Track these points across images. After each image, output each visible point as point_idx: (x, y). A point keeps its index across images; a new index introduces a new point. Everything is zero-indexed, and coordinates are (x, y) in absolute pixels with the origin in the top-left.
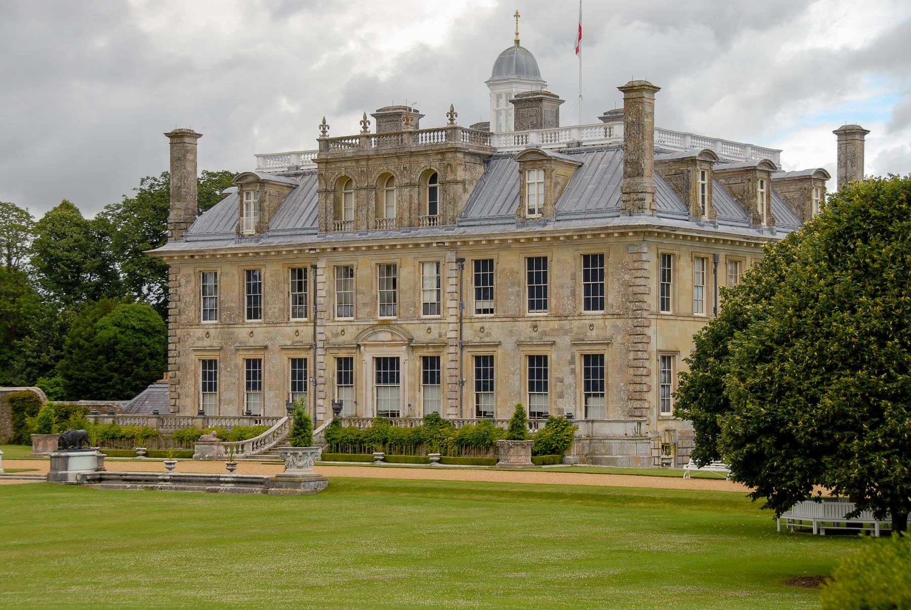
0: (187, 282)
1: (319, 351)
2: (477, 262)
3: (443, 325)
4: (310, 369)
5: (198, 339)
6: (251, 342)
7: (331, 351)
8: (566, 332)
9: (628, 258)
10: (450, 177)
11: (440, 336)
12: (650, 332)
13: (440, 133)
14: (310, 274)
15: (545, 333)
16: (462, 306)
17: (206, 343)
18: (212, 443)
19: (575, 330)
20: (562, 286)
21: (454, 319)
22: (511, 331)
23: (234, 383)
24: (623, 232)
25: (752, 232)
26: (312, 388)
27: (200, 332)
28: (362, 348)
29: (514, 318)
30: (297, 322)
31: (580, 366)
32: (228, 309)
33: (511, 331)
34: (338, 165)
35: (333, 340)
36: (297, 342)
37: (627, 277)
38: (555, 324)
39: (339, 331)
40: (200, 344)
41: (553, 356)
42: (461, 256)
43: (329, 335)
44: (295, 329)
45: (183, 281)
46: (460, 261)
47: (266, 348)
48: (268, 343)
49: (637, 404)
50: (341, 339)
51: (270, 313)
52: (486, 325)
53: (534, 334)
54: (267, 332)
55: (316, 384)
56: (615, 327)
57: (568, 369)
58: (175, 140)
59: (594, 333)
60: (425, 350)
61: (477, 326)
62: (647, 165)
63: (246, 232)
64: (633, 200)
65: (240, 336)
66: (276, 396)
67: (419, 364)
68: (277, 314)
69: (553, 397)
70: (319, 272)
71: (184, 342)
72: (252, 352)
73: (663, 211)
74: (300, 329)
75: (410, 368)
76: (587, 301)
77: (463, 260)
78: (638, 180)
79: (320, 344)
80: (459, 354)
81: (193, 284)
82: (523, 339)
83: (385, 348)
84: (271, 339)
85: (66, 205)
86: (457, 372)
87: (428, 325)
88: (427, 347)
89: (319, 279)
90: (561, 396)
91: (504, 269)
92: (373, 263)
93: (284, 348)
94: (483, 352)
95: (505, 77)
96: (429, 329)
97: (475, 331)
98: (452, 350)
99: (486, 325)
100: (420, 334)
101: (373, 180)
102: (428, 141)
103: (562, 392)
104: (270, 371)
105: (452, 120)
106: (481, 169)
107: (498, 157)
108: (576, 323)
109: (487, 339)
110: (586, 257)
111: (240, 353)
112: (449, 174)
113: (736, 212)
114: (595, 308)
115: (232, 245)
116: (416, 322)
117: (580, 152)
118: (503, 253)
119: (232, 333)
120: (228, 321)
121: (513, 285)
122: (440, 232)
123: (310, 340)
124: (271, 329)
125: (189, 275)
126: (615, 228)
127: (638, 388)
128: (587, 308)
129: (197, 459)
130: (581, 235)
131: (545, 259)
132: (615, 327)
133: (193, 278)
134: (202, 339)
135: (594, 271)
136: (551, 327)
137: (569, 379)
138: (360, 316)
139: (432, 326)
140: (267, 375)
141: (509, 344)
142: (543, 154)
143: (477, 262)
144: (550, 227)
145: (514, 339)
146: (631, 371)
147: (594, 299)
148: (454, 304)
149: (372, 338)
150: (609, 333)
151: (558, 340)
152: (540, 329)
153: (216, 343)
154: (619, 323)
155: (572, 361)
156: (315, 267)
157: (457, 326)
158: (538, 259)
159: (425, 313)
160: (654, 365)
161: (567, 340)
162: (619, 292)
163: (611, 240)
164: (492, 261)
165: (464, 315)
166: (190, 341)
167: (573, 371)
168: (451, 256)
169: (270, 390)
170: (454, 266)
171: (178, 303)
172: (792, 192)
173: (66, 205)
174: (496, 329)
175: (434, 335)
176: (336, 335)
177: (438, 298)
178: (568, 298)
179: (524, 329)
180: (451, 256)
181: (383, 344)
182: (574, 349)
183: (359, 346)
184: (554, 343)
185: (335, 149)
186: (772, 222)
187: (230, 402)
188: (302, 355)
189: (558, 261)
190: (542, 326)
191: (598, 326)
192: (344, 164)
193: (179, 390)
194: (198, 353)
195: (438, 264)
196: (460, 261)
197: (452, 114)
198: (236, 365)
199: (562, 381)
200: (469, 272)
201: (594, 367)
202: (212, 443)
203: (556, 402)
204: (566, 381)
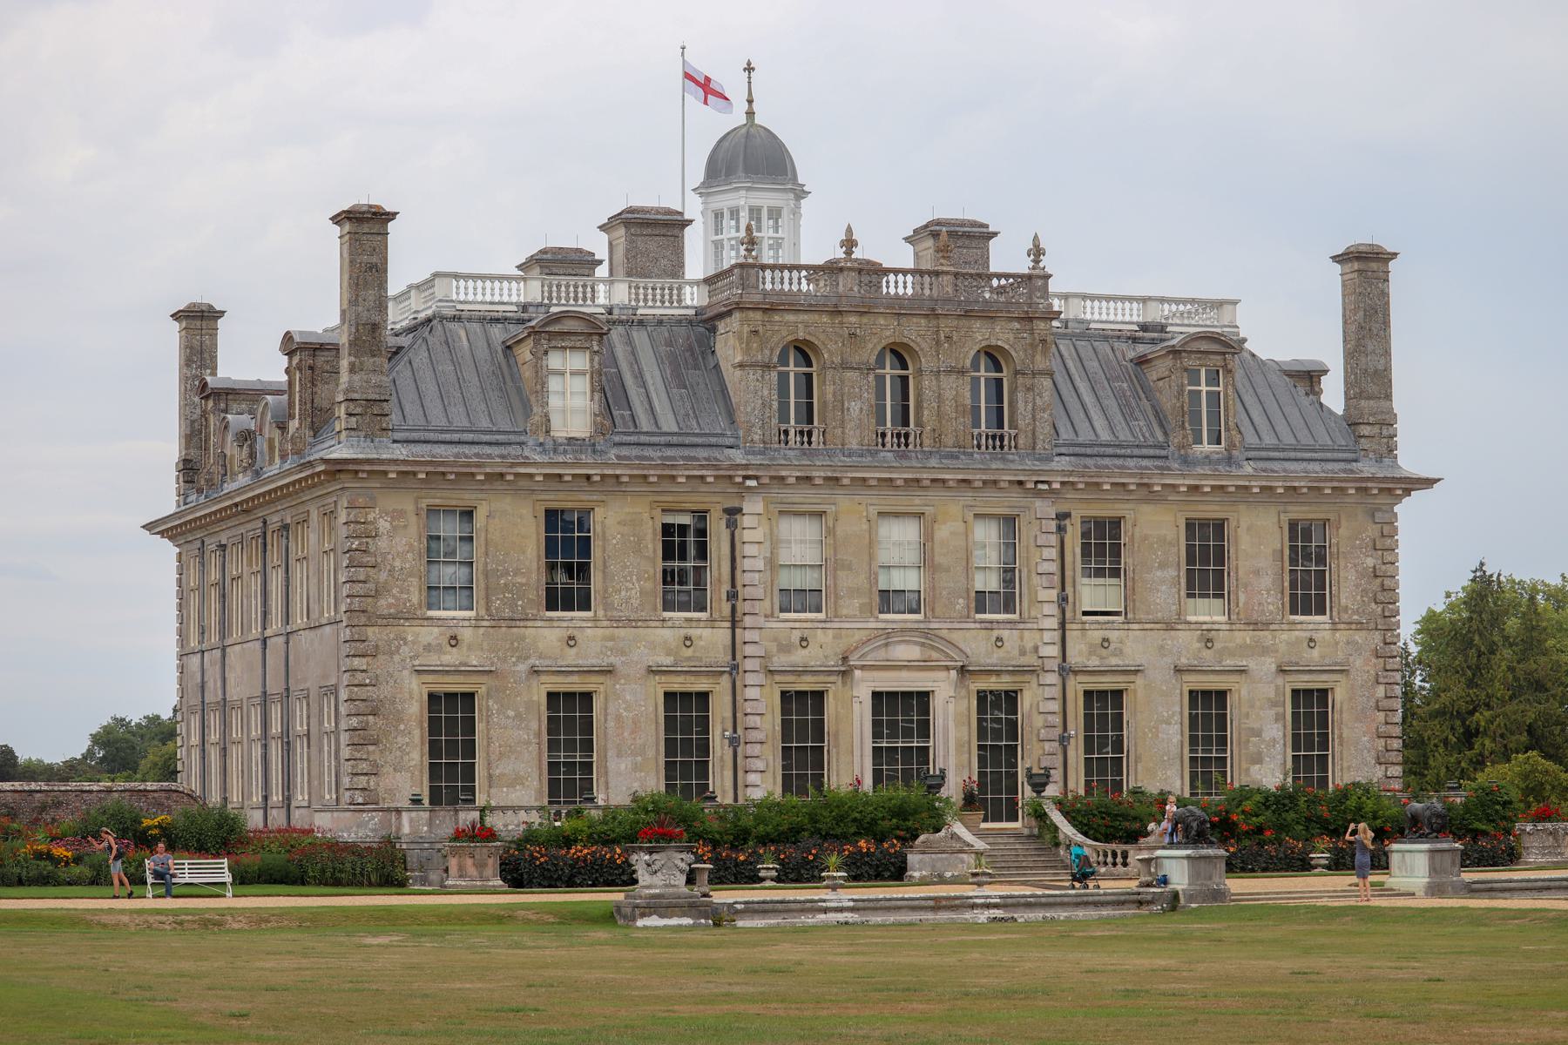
0: (394, 528)
3: (1026, 633)
5: (428, 648)
6: (571, 657)
7: (778, 678)
8: (1265, 651)
9: (1372, 531)
11: (1023, 653)
13: (795, 274)
16: (1063, 599)
17: (451, 658)
19: (1283, 648)
20: (1257, 573)
21: (1053, 623)
22: (1162, 647)
23: (528, 743)
26: (729, 752)
27: (429, 634)
28: (857, 673)
29: (1169, 627)
30: (687, 620)
33: (1162, 647)
34: (790, 317)
35: (779, 661)
36: (689, 659)
37: (1370, 562)
38: (1246, 637)
39: (796, 636)
40: (433, 660)
42: (1064, 508)
43: (773, 647)
44: (683, 632)
45: (384, 525)
46: (1063, 516)
47: (608, 672)
48: (612, 659)
50: (799, 657)
51: (616, 599)
52: (1113, 635)
53: (1207, 654)
54: (612, 638)
55: (734, 742)
58: (366, 228)
59: (1316, 653)
60: (993, 679)
61: (1096, 636)
65: (540, 645)
66: (636, 768)
68: (635, 602)
69: (1244, 766)
70: (747, 521)
71: (392, 654)
72: (575, 678)
74: (693, 632)
77: (1067, 515)
78: (1383, 403)
79: (749, 665)
80: (1059, 688)
81: (413, 530)
82: (1184, 661)
83: (904, 674)
86: (1057, 720)
87: (995, 633)
88: (998, 673)
89: (748, 535)
91: (1145, 538)
93: (652, 671)
94: (1106, 683)
96: (999, 639)
97: (1091, 645)
101: (869, 353)
102: (927, 292)
103: (1260, 753)
104: (619, 718)
105: (1037, 261)
108: (1285, 636)
109: (1114, 661)
110: (1293, 525)
111: (544, 678)
112: (1038, 358)
116: (972, 626)
118: (1146, 508)
119: (523, 638)
120: (507, 613)
121: (1162, 566)
123: (724, 658)
124: (622, 632)
125: (401, 514)
133: (413, 519)
134: (439, 649)
136: (1238, 641)
138: (938, 611)
139: (1005, 634)
140: (611, 724)
145: (1169, 661)
146: (1381, 716)
148: (1053, 594)
149: (882, 654)
150: (1340, 656)
151: (1251, 664)
152: (1218, 645)
154: (1359, 637)
156: (733, 513)
157: (1056, 636)
161: (1269, 664)
162: (1357, 586)
165: (1068, 615)
166: (405, 650)
168: (1046, 509)
169: (619, 755)
170: (1053, 526)
171: (371, 571)
174: (1134, 646)
176: (785, 648)
178: (1268, 591)
179: (1185, 644)
180: (1046, 509)
182: (1280, 681)
183: (846, 674)
184: (1242, 672)
187: (516, 781)
188: (700, 685)
189: (1249, 529)
192: (805, 317)
193: (377, 757)
194: (430, 678)
197: (849, 244)
203: (1248, 770)
204: (1267, 736)
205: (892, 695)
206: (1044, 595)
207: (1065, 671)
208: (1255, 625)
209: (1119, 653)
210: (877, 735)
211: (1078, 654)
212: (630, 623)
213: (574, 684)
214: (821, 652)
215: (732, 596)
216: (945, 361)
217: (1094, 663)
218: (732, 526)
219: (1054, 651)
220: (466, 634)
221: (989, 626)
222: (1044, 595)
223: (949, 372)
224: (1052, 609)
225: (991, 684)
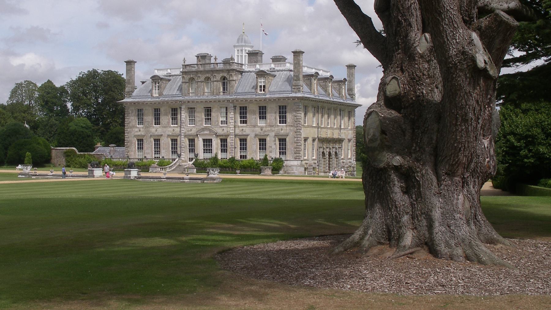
1: (182, 137)
2: (241, 107)
4: (178, 142)
6: (156, 133)
8: (273, 131)
10: (231, 79)
12: (301, 131)
14: (179, 110)
15: (265, 131)
16: (235, 122)
17: (139, 133)
18: (156, 167)
24: (294, 98)
25: (328, 99)
27: (137, 130)
29: (254, 126)
31: (278, 143)
32: (148, 122)
35: (187, 133)
40: (137, 134)
41: (268, 139)
45: (130, 112)
47: (162, 135)
49: (297, 155)
50: (190, 132)
52: (244, 128)
55: (181, 147)
56: (290, 129)
57: (273, 143)
62: (301, 77)
63: (154, 95)
64: (297, 88)
67: (219, 141)
73: (304, 92)
75: (216, 144)
76: (280, 121)
78: (298, 82)
79: (182, 134)
84: (164, 132)
85: (49, 81)
90: (271, 152)
92: (203, 107)
93: (168, 136)
95: (240, 44)
98: (232, 136)
99: (244, 128)
100: (220, 131)
106: (240, 76)
107: (245, 72)
110: (280, 107)
113: (323, 92)
114: (283, 123)
115: (150, 100)
117: (275, 71)
122: (228, 97)
126: (291, 97)
127: (298, 149)
128: (280, 123)
129: (151, 172)
130: (279, 99)
131: (265, 107)
132: (290, 129)
135: (283, 111)
137: (274, 147)
141: (253, 135)
142: (265, 72)
143: (241, 107)
144: (268, 96)
145: (254, 133)
147: (283, 120)
148: (233, 121)
153: (143, 134)
154: (292, 128)
155: (275, 141)
157: (234, 129)
158: (263, 107)
159: (222, 124)
160: (303, 142)
161: (273, 134)
163: (289, 101)
164: (246, 107)
167: (275, 144)
172: (336, 85)
173: (49, 81)
174: (247, 130)
175: (225, 131)
177: (227, 119)
179: (258, 130)
181: (206, 135)
185: (188, 69)
186: (333, 95)
187: (148, 153)
190: (264, 129)
191: (283, 129)
195: (227, 108)
196: (235, 107)
198: (151, 141)
199: (271, 147)
200: (238, 111)
201: (283, 141)
202: (156, 167)
205: (207, 139)
206: (231, 121)
207: (236, 136)
208: (271, 126)
209: (245, 132)
210: (189, 147)
211: (238, 131)
212: (165, 127)
213: (157, 138)
214: (194, 131)
215: (181, 122)
216: (215, 79)
217: (241, 133)
218: (181, 110)
219: (233, 131)
220: (141, 129)
221: (221, 127)
222: (231, 121)
223: (215, 81)
224: (233, 124)
225: (222, 137)
